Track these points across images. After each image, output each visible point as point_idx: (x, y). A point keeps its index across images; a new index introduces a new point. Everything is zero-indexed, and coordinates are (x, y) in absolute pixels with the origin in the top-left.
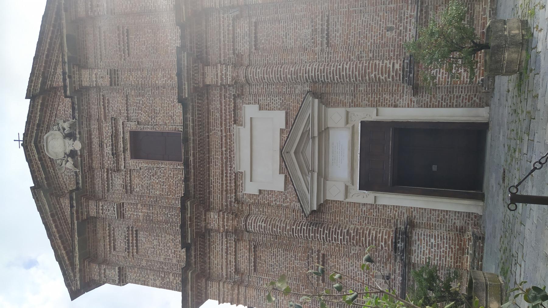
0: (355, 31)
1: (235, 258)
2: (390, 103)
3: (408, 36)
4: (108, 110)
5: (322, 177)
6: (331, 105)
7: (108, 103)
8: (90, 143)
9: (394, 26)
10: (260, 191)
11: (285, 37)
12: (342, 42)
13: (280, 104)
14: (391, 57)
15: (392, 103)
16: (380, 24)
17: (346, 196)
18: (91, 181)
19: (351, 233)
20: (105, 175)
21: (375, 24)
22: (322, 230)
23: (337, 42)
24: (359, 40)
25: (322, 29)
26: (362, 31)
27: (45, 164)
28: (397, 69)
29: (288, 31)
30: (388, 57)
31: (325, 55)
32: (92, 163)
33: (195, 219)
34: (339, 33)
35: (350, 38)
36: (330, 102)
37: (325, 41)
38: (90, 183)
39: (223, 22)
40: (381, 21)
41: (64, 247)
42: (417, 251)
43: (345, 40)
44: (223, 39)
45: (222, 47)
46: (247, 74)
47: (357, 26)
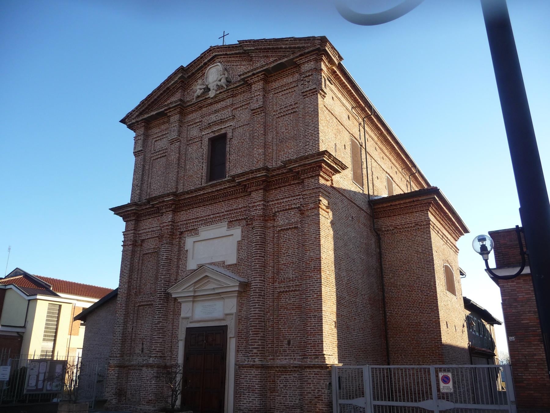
0: (289, 314)
1: (149, 238)
2: (240, 347)
3: (282, 357)
4: (241, 110)
5: (193, 298)
6: (240, 300)
7: (245, 108)
8: (216, 102)
9: (291, 346)
10: (187, 251)
11: (287, 255)
12: (282, 304)
13: (242, 258)
14: (268, 346)
15: (240, 348)
16: (292, 335)
17: (183, 318)
18: (193, 111)
19: (159, 324)
20: (198, 120)
21: (293, 330)
22: (161, 303)
23: (282, 300)
24: (282, 318)
25: (290, 286)
26: (289, 320)
27: (203, 69)
28: (253, 351)
29: (291, 257)
30: (268, 343)
31: (272, 292)
32: (204, 107)
33: (165, 204)
34: (288, 301)
35: (284, 310)
36: (242, 299)
37: (282, 290)
38: (192, 110)
39: (297, 199)
40: (295, 335)
41: (150, 104)
42: (148, 371)
43: (283, 306)
44: (285, 201)
45: (279, 201)
46: (256, 228)
47: (293, 316)
